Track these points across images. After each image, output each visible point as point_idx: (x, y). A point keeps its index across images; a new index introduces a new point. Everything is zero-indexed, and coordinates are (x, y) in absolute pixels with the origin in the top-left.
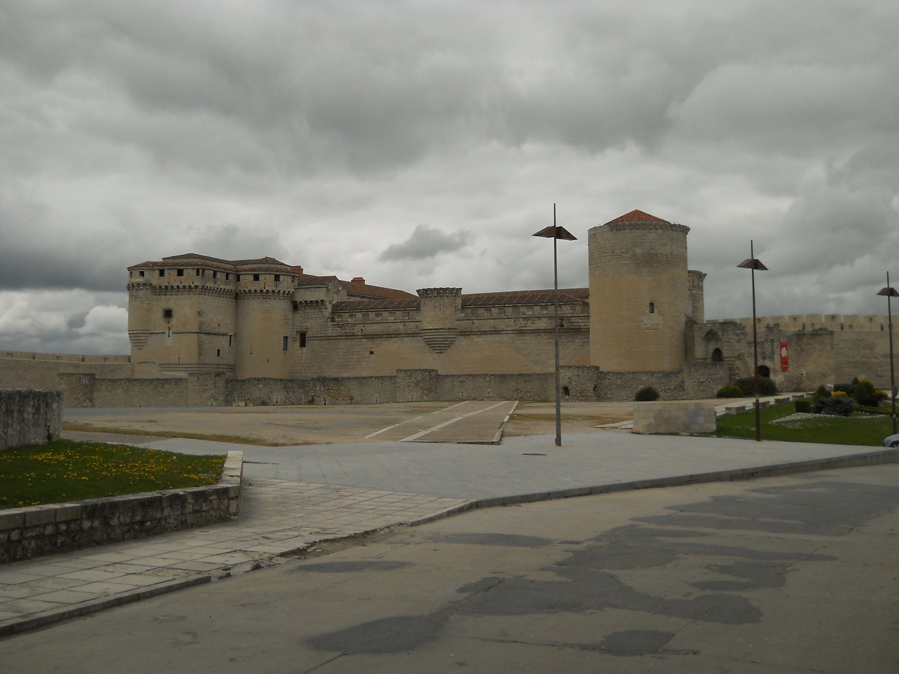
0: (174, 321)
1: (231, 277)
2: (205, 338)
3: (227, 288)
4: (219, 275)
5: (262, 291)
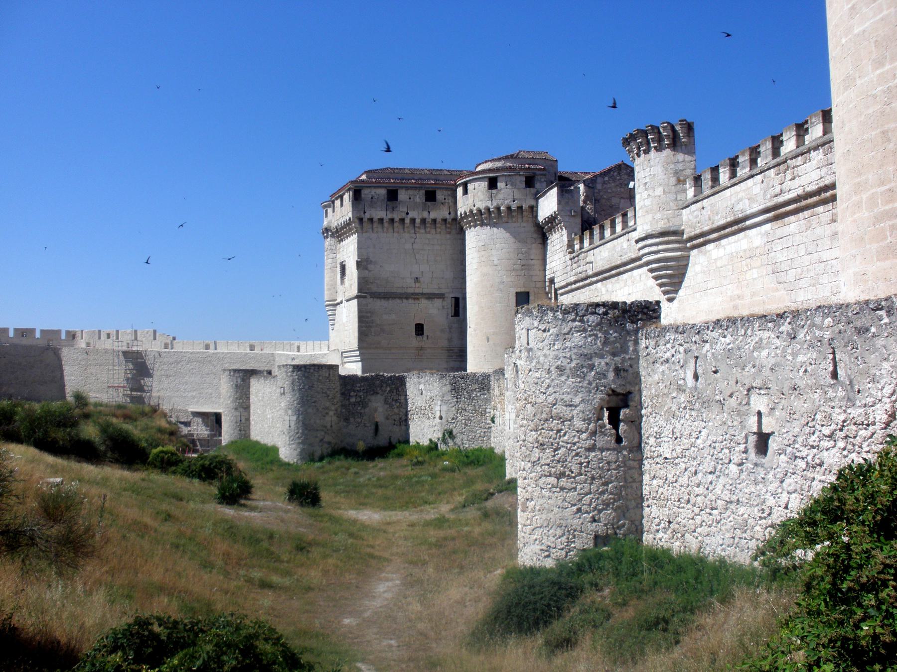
0: (346, 280)
1: (440, 196)
2: (378, 305)
3: (433, 215)
4: (402, 195)
5: (471, 211)
